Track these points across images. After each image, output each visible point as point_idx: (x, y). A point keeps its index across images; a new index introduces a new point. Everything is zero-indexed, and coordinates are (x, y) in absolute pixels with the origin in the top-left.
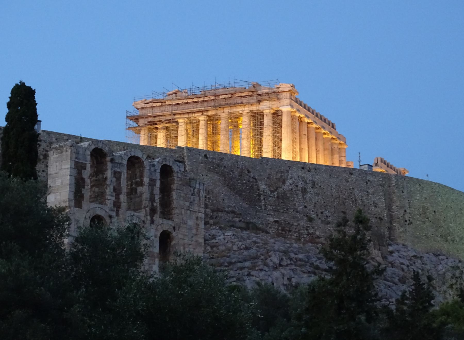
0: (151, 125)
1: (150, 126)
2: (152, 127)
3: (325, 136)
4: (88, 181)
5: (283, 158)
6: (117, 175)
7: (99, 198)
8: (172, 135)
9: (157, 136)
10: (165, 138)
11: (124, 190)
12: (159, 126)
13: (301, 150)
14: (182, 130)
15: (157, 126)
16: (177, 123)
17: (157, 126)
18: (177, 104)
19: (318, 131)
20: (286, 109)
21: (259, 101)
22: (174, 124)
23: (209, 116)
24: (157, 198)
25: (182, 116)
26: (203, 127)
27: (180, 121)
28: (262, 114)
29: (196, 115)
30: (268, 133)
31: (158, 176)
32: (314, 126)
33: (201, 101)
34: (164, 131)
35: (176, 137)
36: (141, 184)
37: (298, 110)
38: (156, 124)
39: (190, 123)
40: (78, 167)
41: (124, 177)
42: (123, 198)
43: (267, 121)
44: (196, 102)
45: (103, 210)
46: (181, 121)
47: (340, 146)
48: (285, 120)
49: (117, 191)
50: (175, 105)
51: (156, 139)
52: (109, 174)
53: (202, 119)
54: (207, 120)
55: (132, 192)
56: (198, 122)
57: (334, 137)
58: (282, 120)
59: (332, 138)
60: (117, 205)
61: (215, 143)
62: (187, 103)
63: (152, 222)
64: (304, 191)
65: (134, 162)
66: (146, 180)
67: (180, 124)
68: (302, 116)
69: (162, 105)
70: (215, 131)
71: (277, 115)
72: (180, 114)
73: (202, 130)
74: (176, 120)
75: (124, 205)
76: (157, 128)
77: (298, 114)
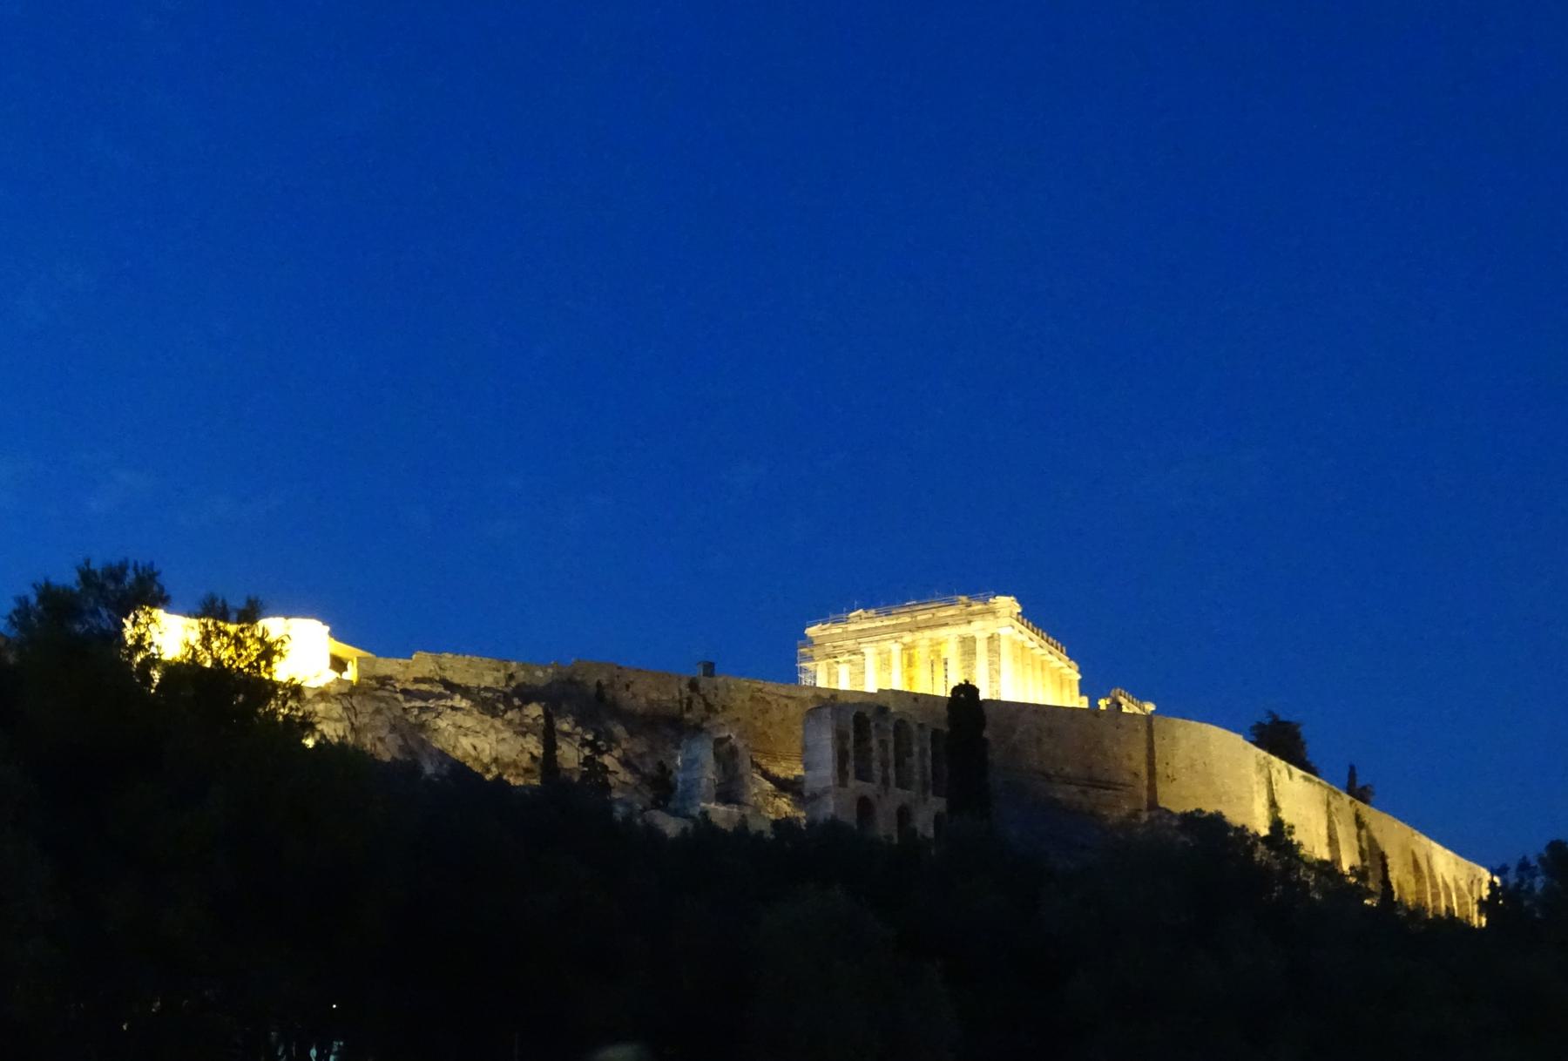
4: (852, 754)
6: (883, 743)
7: (863, 774)
11: (892, 763)
12: (840, 659)
24: (929, 770)
28: (973, 639)
31: (929, 746)
32: (1040, 651)
36: (910, 754)
40: (840, 737)
41: (891, 746)
42: (892, 772)
43: (981, 647)
45: (869, 789)
46: (870, 650)
48: (1005, 647)
49: (884, 765)
52: (874, 743)
53: (896, 648)
55: (899, 763)
60: (885, 781)
61: (911, 679)
63: (926, 800)
64: (1039, 740)
65: (901, 726)
66: (916, 749)
70: (910, 664)
75: (892, 783)
77: (1020, 637)
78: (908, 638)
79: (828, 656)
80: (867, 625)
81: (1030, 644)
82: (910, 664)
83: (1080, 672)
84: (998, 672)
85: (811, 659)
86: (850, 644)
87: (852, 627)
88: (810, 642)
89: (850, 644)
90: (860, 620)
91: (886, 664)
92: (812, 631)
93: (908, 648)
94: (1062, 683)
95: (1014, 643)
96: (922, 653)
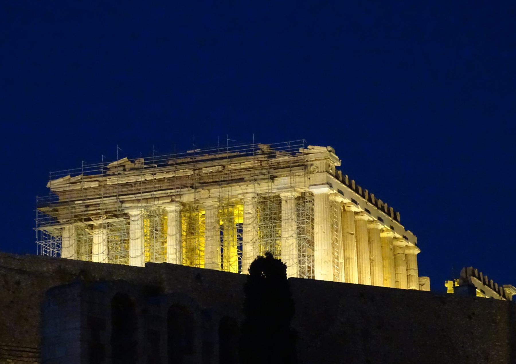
0: (81, 220)
1: (79, 224)
2: (82, 224)
3: (383, 235)
5: (318, 277)
8: (120, 240)
9: (91, 240)
10: (105, 243)
12: (96, 223)
13: (347, 259)
14: (137, 229)
15: (91, 223)
16: (126, 216)
17: (91, 223)
18: (127, 184)
19: (372, 226)
20: (320, 191)
21: (272, 178)
22: (122, 219)
23: (183, 205)
25: (136, 205)
26: (174, 224)
27: (133, 212)
28: (278, 200)
29: (161, 202)
30: (291, 233)
32: (366, 217)
33: (169, 179)
34: (105, 231)
35: (126, 241)
37: (340, 192)
38: (90, 220)
39: (150, 216)
43: (288, 210)
44: (160, 180)
47: (407, 252)
48: (319, 211)
50: (122, 185)
51: (91, 246)
54: (181, 211)
56: (164, 213)
57: (397, 236)
58: (312, 210)
59: (395, 238)
61: (192, 250)
62: (145, 182)
67: (133, 219)
68: (347, 201)
69: (100, 186)
70: (192, 230)
71: (303, 200)
72: (133, 201)
73: (171, 229)
74: (126, 211)
76: (92, 227)
77: (339, 199)
78: (188, 197)
79: (78, 218)
80: (132, 179)
81: (354, 208)
82: (192, 230)
83: (418, 245)
84: (311, 243)
85: (55, 221)
86: (109, 202)
87: (111, 181)
88: (53, 198)
89: (109, 202)
90: (123, 173)
91: (156, 232)
92: (56, 184)
93: (188, 211)
94: (395, 258)
95: (332, 205)
96: (202, 216)
